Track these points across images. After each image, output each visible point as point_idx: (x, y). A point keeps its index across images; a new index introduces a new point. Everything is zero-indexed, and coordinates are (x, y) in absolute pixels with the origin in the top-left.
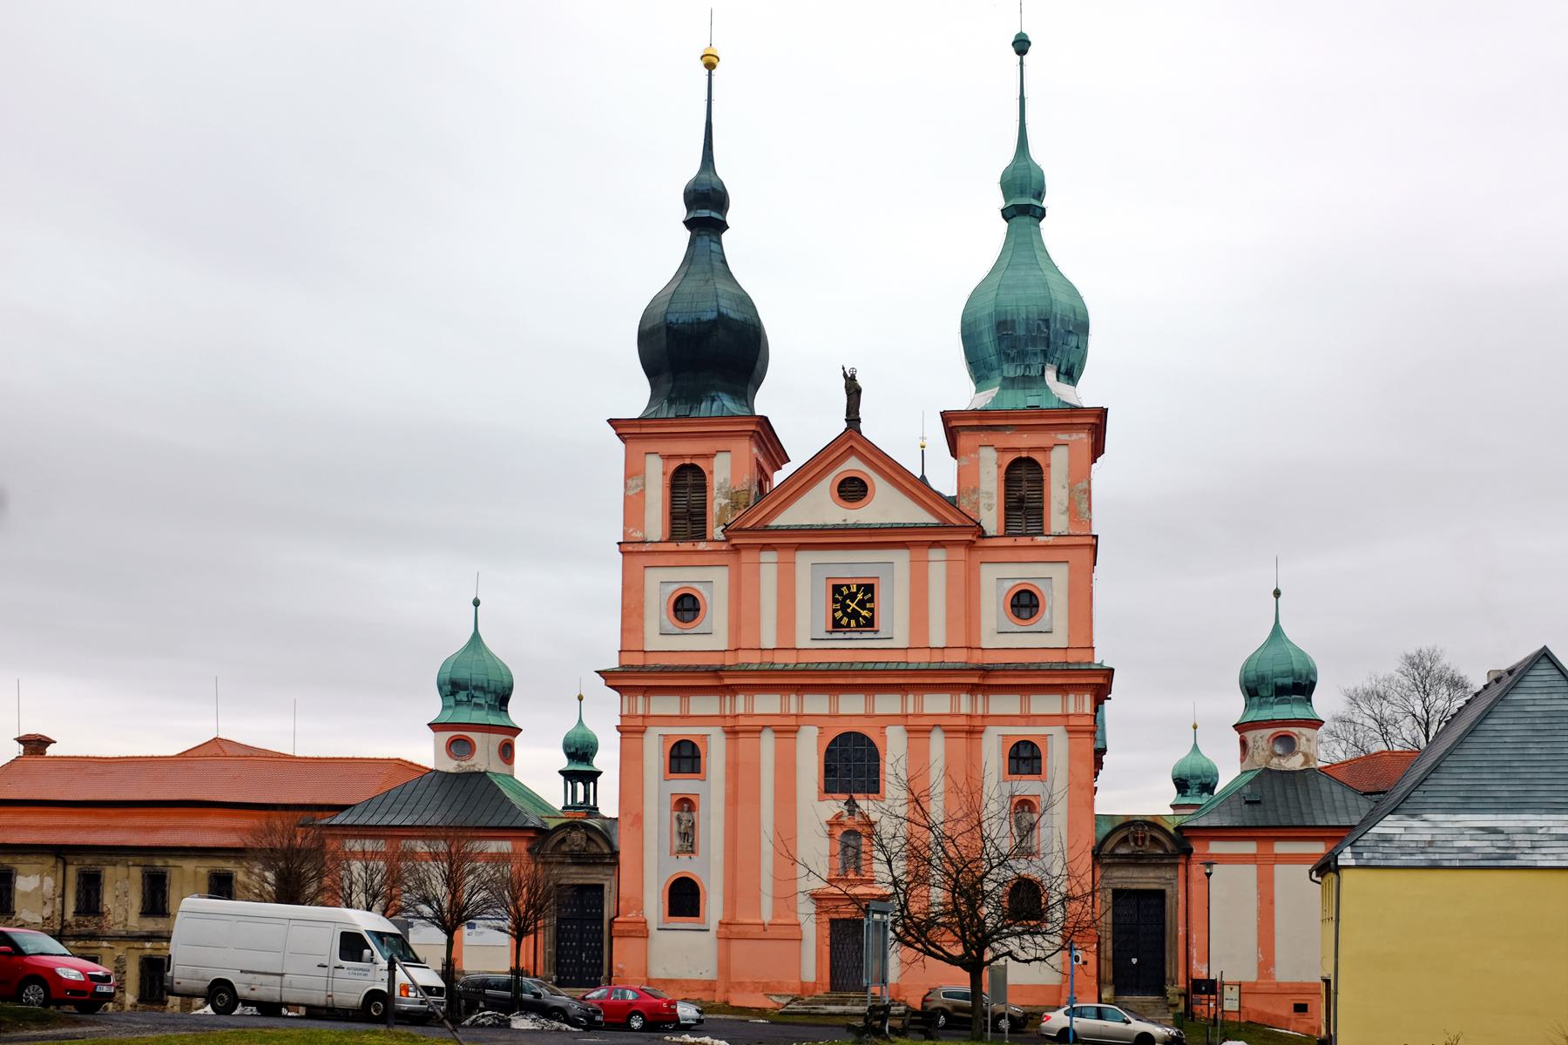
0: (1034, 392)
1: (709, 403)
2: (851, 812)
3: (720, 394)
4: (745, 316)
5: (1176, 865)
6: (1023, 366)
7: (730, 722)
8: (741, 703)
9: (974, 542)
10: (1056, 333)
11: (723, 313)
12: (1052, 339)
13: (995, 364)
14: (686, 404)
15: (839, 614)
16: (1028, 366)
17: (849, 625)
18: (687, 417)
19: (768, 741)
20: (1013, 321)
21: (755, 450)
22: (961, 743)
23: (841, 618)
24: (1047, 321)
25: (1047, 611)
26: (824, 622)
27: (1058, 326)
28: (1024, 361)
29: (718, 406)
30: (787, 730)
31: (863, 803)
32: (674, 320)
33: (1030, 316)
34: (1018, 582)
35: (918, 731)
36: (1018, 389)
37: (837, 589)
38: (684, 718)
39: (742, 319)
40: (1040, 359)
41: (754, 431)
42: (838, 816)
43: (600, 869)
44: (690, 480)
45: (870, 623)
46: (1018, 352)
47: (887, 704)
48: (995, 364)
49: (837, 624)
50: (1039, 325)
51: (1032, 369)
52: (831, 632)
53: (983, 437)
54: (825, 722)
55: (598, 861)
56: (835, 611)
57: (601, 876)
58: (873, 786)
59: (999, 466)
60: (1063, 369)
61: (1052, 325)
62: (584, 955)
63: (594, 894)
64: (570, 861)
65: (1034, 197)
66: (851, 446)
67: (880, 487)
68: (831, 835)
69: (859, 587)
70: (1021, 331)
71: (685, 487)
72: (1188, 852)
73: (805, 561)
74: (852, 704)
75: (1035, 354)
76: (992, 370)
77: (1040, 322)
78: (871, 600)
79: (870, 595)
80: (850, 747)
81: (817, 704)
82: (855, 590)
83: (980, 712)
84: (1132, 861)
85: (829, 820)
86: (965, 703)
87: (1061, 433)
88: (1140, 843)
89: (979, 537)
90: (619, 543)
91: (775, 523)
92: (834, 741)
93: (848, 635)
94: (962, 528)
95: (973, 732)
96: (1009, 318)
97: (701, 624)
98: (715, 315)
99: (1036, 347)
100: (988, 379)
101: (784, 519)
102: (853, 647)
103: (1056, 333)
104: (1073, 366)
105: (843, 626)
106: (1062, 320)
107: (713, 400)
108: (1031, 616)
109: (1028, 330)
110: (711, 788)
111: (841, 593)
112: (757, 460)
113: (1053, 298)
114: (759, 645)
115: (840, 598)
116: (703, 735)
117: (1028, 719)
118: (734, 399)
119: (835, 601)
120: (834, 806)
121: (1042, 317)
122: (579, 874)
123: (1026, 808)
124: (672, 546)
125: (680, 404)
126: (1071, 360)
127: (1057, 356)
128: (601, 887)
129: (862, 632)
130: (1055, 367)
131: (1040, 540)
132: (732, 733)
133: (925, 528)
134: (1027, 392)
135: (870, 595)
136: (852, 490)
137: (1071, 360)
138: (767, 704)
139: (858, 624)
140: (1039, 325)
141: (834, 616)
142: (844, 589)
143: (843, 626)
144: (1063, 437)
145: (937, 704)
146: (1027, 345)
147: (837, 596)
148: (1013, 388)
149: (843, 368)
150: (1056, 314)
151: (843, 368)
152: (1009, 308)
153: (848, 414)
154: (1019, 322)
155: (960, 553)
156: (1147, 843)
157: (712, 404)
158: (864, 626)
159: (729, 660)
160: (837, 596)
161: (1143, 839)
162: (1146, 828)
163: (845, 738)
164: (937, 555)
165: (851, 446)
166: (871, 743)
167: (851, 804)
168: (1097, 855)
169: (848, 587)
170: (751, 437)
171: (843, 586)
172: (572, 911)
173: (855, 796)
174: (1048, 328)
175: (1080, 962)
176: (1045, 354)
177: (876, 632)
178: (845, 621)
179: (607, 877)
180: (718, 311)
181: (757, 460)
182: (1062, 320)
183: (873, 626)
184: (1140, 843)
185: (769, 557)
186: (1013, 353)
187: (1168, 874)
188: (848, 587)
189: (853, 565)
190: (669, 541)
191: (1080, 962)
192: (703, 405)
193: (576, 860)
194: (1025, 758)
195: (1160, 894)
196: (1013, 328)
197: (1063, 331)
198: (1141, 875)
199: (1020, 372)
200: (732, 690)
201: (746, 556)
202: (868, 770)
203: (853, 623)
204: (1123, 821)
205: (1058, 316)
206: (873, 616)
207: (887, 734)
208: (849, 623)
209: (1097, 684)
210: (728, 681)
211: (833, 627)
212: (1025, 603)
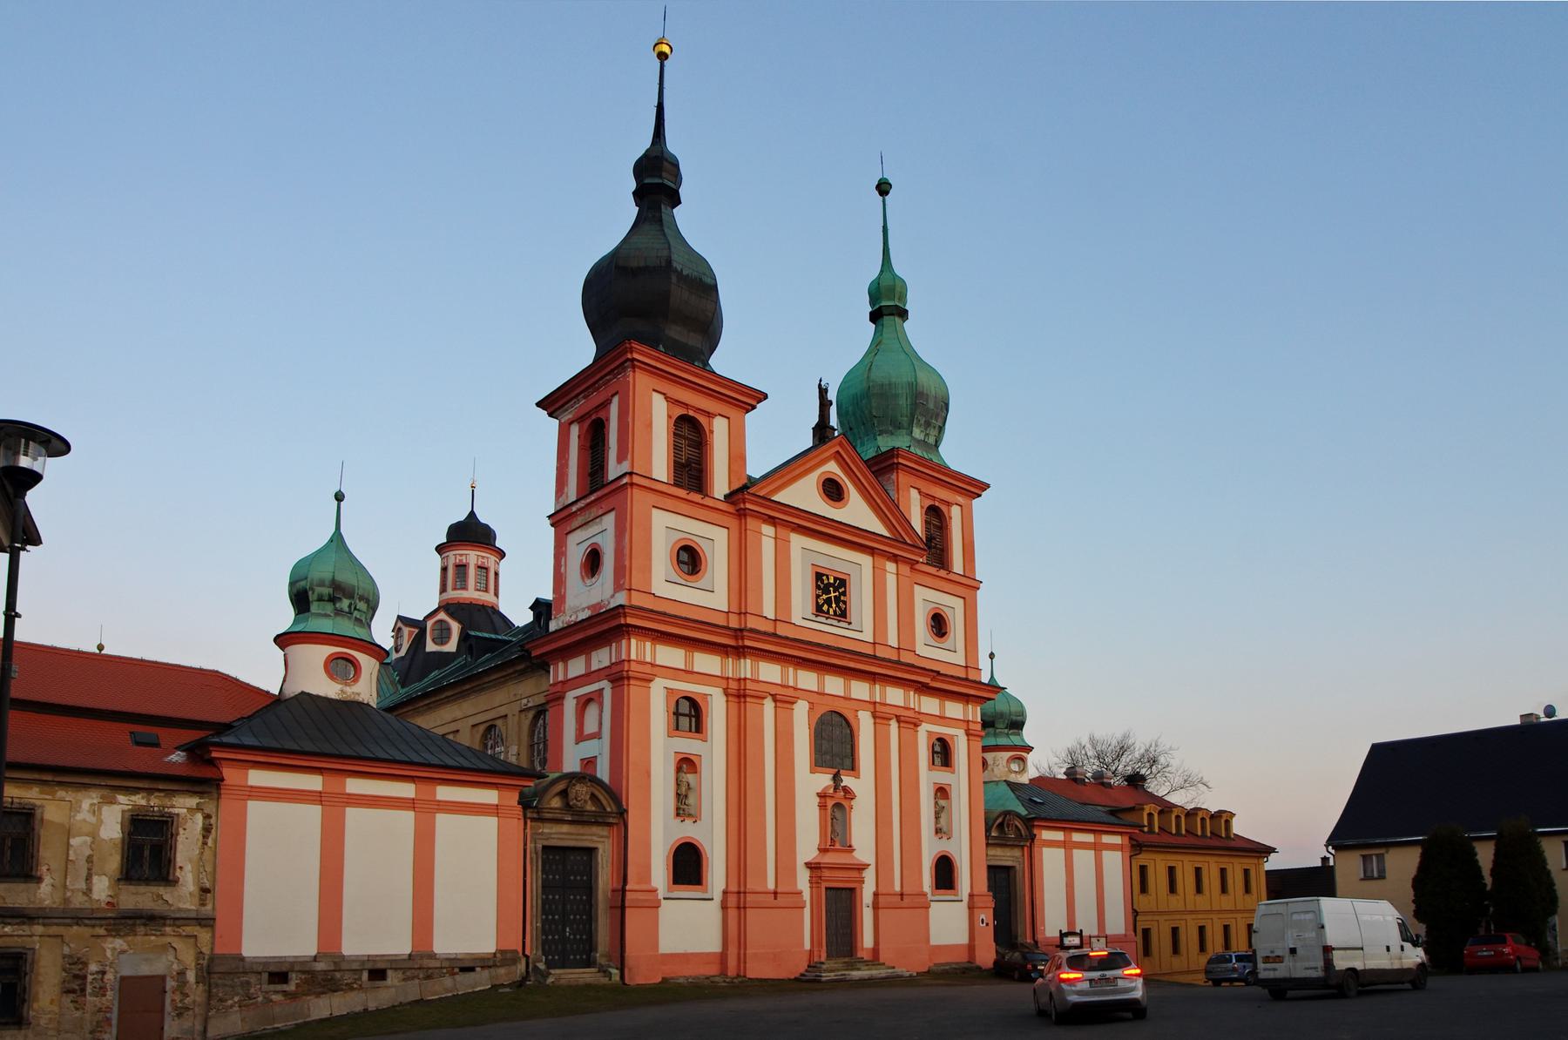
2: (836, 788)
5: (1023, 847)
7: (733, 685)
8: (746, 667)
13: (905, 425)
16: (927, 435)
17: (828, 612)
19: (769, 705)
20: (927, 395)
22: (907, 733)
23: (823, 605)
25: (952, 634)
28: (926, 429)
30: (784, 700)
31: (847, 781)
35: (880, 715)
37: (819, 576)
38: (688, 673)
42: (827, 788)
43: (595, 829)
46: (925, 421)
47: (860, 689)
48: (905, 425)
49: (819, 609)
52: (817, 616)
54: (816, 699)
55: (600, 820)
56: (818, 596)
57: (595, 838)
58: (853, 768)
59: (922, 507)
62: (568, 930)
63: (579, 858)
64: (570, 819)
66: (838, 452)
68: (822, 806)
70: (931, 405)
72: (1033, 838)
73: (798, 542)
75: (934, 427)
78: (844, 594)
79: (843, 589)
81: (807, 680)
84: (1003, 842)
85: (819, 791)
91: (776, 498)
93: (829, 621)
96: (925, 392)
102: (828, 630)
105: (823, 612)
109: (935, 406)
111: (822, 581)
115: (822, 586)
116: (705, 694)
117: (942, 719)
119: (818, 587)
120: (824, 780)
122: (572, 834)
128: (595, 849)
129: (839, 621)
132: (739, 694)
135: (843, 589)
138: (770, 672)
141: (817, 602)
142: (825, 578)
143: (823, 612)
145: (895, 696)
146: (932, 418)
152: (925, 384)
155: (905, 569)
158: (839, 616)
159: (734, 623)
160: (819, 583)
165: (838, 452)
167: (836, 778)
171: (824, 575)
172: (581, 879)
177: (850, 623)
179: (601, 839)
185: (768, 530)
187: (1017, 853)
188: (828, 579)
193: (576, 818)
195: (1008, 869)
198: (1002, 854)
200: (739, 652)
201: (751, 523)
208: (828, 610)
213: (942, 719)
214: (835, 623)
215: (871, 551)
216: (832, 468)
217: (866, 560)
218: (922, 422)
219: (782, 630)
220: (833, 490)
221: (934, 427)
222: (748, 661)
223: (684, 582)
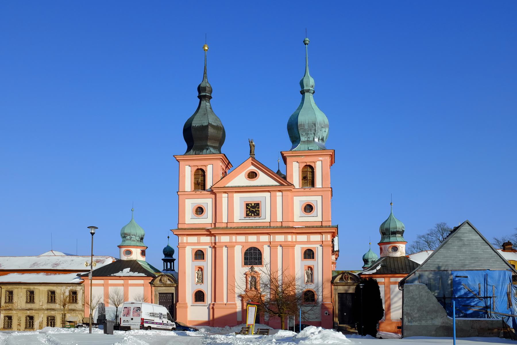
0: (311, 145)
1: (206, 150)
3: (209, 147)
4: (218, 125)
6: (307, 138)
9: (292, 190)
10: (318, 128)
11: (210, 123)
12: (316, 129)
14: (199, 151)
15: (248, 212)
18: (199, 154)
19: (225, 250)
20: (304, 124)
21: (221, 164)
23: (249, 213)
24: (315, 125)
25: (316, 210)
26: (244, 214)
27: (318, 125)
29: (209, 151)
31: (257, 268)
32: (194, 126)
33: (309, 123)
34: (306, 202)
36: (306, 144)
37: (247, 205)
39: (217, 125)
40: (313, 135)
41: (220, 158)
44: (200, 172)
45: (258, 215)
47: (264, 238)
49: (247, 215)
50: (312, 125)
51: (310, 138)
52: (245, 217)
53: (294, 158)
56: (247, 211)
60: (320, 138)
61: (317, 125)
65: (311, 87)
67: (261, 174)
69: (255, 204)
71: (199, 175)
73: (237, 197)
74: (252, 239)
75: (311, 134)
76: (297, 139)
77: (313, 125)
80: (252, 251)
81: (241, 239)
82: (253, 205)
83: (294, 240)
86: (289, 238)
87: (320, 158)
88: (346, 279)
89: (293, 188)
90: (177, 192)
92: (247, 250)
94: (288, 185)
95: (292, 245)
96: (302, 124)
97: (204, 215)
98: (207, 124)
99: (311, 132)
100: (296, 141)
101: (230, 184)
103: (318, 128)
104: (323, 137)
105: (250, 216)
106: (320, 124)
107: (207, 149)
108: (310, 212)
109: (309, 127)
110: (207, 264)
111: (249, 206)
112: (221, 166)
113: (317, 117)
114: (222, 221)
118: (214, 149)
119: (247, 208)
120: (247, 269)
121: (313, 123)
123: (310, 269)
124: (194, 193)
125: (197, 151)
126: (323, 135)
127: (318, 134)
129: (255, 217)
130: (318, 138)
131: (313, 189)
133: (276, 186)
134: (309, 145)
136: (252, 175)
137: (323, 135)
138: (225, 239)
139: (254, 215)
140: (312, 125)
141: (247, 213)
144: (321, 158)
145: (280, 238)
146: (308, 131)
147: (248, 207)
148: (304, 144)
149: (249, 139)
150: (318, 122)
151: (249, 139)
152: (302, 121)
153: (251, 152)
154: (306, 125)
155: (289, 193)
156: (349, 279)
157: (207, 150)
158: (256, 215)
160: (248, 207)
161: (348, 278)
162: (348, 274)
163: (251, 249)
164: (279, 194)
166: (259, 250)
167: (252, 268)
168: (332, 282)
169: (251, 204)
170: (219, 160)
171: (249, 204)
173: (254, 266)
174: (315, 126)
175: (327, 315)
176: (314, 134)
178: (250, 214)
180: (209, 123)
181: (221, 166)
182: (320, 124)
183: (259, 216)
184: (346, 279)
185: (225, 195)
186: (304, 134)
189: (253, 197)
190: (194, 191)
191: (327, 315)
192: (204, 151)
194: (309, 254)
196: (304, 126)
197: (320, 127)
199: (306, 139)
202: (258, 258)
203: (253, 215)
204: (341, 272)
205: (319, 123)
206: (259, 212)
207: (264, 247)
209: (332, 232)
210: (212, 232)
211: (246, 216)
212: (309, 208)
213: (308, 242)
214: (253, 218)
215: (269, 191)
216: (252, 168)
217: (268, 195)
218: (304, 134)
219: (229, 225)
220: (252, 175)
221: (311, 134)
222: (213, 237)
223: (197, 218)
